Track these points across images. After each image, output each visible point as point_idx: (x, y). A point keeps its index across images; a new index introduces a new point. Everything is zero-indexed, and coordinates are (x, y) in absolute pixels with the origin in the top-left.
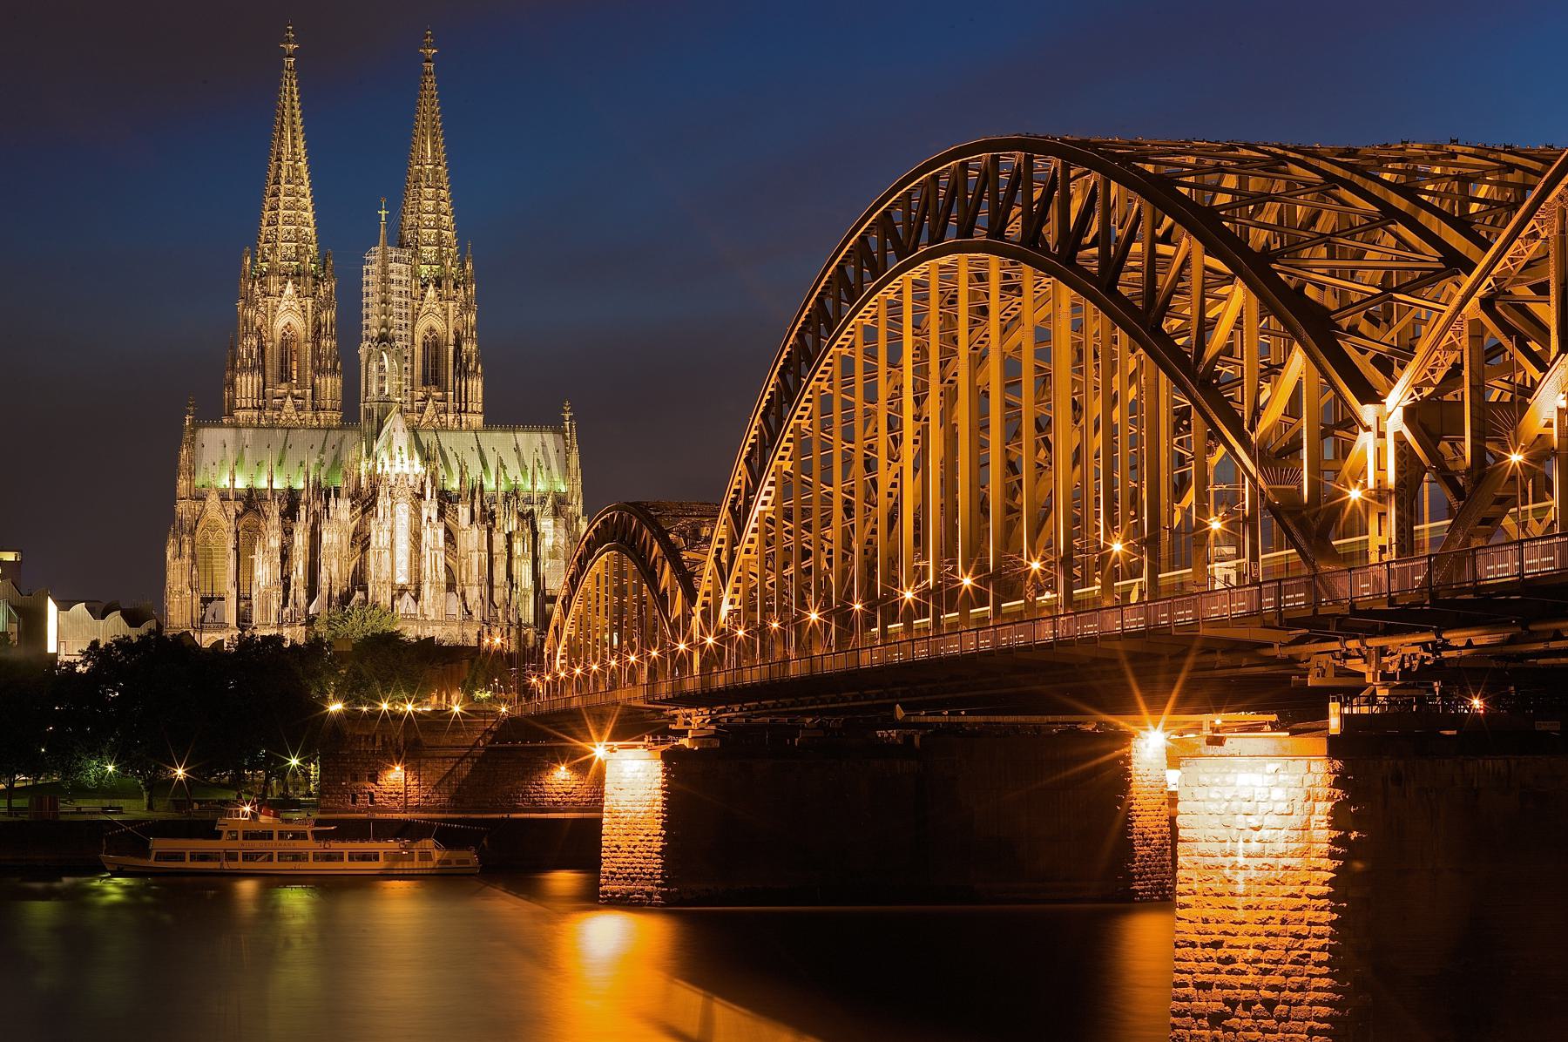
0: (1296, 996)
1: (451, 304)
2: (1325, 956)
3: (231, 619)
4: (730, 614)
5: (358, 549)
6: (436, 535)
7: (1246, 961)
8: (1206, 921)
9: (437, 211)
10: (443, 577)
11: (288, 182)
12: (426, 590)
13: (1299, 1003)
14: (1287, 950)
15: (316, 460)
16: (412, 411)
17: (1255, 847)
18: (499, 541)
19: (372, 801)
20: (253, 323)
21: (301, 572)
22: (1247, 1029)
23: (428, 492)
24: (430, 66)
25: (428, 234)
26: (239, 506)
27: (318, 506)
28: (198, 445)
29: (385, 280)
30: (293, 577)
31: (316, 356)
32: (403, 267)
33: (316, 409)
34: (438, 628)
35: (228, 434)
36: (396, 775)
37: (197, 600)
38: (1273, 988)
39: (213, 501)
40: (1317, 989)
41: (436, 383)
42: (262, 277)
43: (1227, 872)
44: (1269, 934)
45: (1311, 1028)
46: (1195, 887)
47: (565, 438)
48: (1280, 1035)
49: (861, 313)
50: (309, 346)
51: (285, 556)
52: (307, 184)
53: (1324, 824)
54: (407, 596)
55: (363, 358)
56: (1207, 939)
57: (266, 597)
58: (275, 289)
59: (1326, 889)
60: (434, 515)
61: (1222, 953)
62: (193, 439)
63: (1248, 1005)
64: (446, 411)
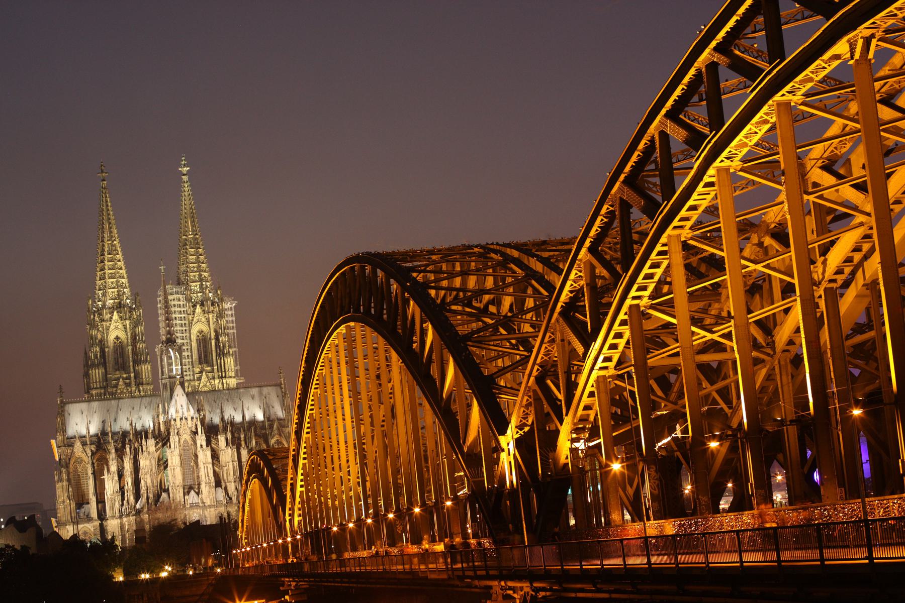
1: (211, 315)
3: (94, 514)
4: (299, 522)
5: (162, 468)
6: (206, 455)
9: (198, 262)
10: (213, 479)
11: (109, 254)
12: (203, 486)
15: (136, 416)
16: (194, 380)
18: (244, 453)
20: (96, 338)
21: (130, 484)
24: (185, 178)
25: (194, 275)
26: (93, 448)
27: (136, 445)
28: (66, 415)
29: (167, 306)
30: (126, 488)
31: (135, 353)
32: (181, 296)
33: (139, 384)
34: (213, 509)
35: (84, 406)
37: (73, 506)
39: (78, 445)
41: (206, 362)
42: (99, 311)
47: (281, 388)
49: (325, 352)
50: (130, 348)
51: (121, 475)
52: (120, 254)
54: (192, 492)
55: (158, 353)
57: (112, 500)
58: (107, 317)
60: (204, 444)
62: (63, 411)
64: (214, 378)
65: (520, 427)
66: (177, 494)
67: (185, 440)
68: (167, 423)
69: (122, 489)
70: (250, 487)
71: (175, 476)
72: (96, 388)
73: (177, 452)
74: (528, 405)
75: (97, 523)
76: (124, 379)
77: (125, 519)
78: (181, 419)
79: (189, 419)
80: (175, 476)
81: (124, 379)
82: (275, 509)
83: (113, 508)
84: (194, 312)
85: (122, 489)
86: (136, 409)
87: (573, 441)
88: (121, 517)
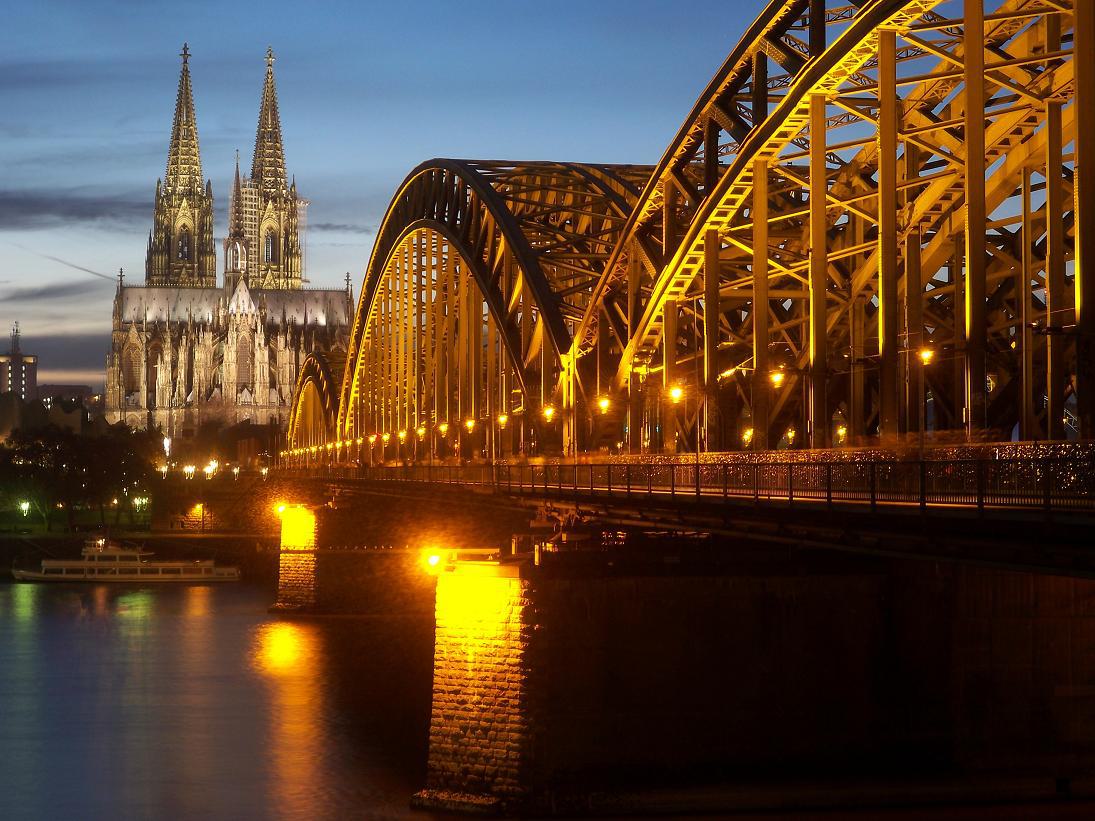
0: (500, 726)
2: (517, 702)
3: (143, 402)
4: (351, 429)
7: (473, 703)
8: (451, 677)
10: (267, 380)
12: (257, 386)
13: (502, 730)
14: (496, 697)
17: (478, 634)
19: (182, 527)
21: (183, 376)
22: (473, 745)
23: (259, 328)
34: (264, 410)
36: (198, 510)
37: (123, 392)
38: (486, 720)
39: (134, 330)
40: (512, 722)
43: (463, 648)
44: (486, 687)
45: (508, 746)
46: (445, 655)
48: (491, 749)
50: (196, 237)
53: (518, 620)
56: (451, 688)
57: (163, 390)
58: (175, 203)
59: (518, 660)
60: (263, 342)
61: (459, 697)
63: (474, 730)
64: (279, 277)
65: (583, 347)
66: (231, 391)
67: (244, 337)
68: (227, 318)
69: (174, 379)
70: (304, 390)
71: (230, 372)
72: (158, 275)
73: (234, 348)
74: (593, 326)
75: (146, 412)
76: (187, 268)
77: (174, 411)
78: (242, 315)
79: (250, 316)
80: (230, 372)
81: (187, 268)
82: (327, 413)
83: (162, 399)
84: (265, 207)
85: (174, 379)
86: (197, 300)
87: (635, 365)
88: (170, 408)
